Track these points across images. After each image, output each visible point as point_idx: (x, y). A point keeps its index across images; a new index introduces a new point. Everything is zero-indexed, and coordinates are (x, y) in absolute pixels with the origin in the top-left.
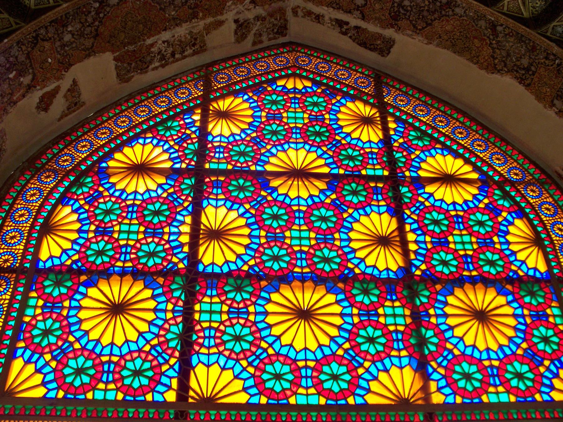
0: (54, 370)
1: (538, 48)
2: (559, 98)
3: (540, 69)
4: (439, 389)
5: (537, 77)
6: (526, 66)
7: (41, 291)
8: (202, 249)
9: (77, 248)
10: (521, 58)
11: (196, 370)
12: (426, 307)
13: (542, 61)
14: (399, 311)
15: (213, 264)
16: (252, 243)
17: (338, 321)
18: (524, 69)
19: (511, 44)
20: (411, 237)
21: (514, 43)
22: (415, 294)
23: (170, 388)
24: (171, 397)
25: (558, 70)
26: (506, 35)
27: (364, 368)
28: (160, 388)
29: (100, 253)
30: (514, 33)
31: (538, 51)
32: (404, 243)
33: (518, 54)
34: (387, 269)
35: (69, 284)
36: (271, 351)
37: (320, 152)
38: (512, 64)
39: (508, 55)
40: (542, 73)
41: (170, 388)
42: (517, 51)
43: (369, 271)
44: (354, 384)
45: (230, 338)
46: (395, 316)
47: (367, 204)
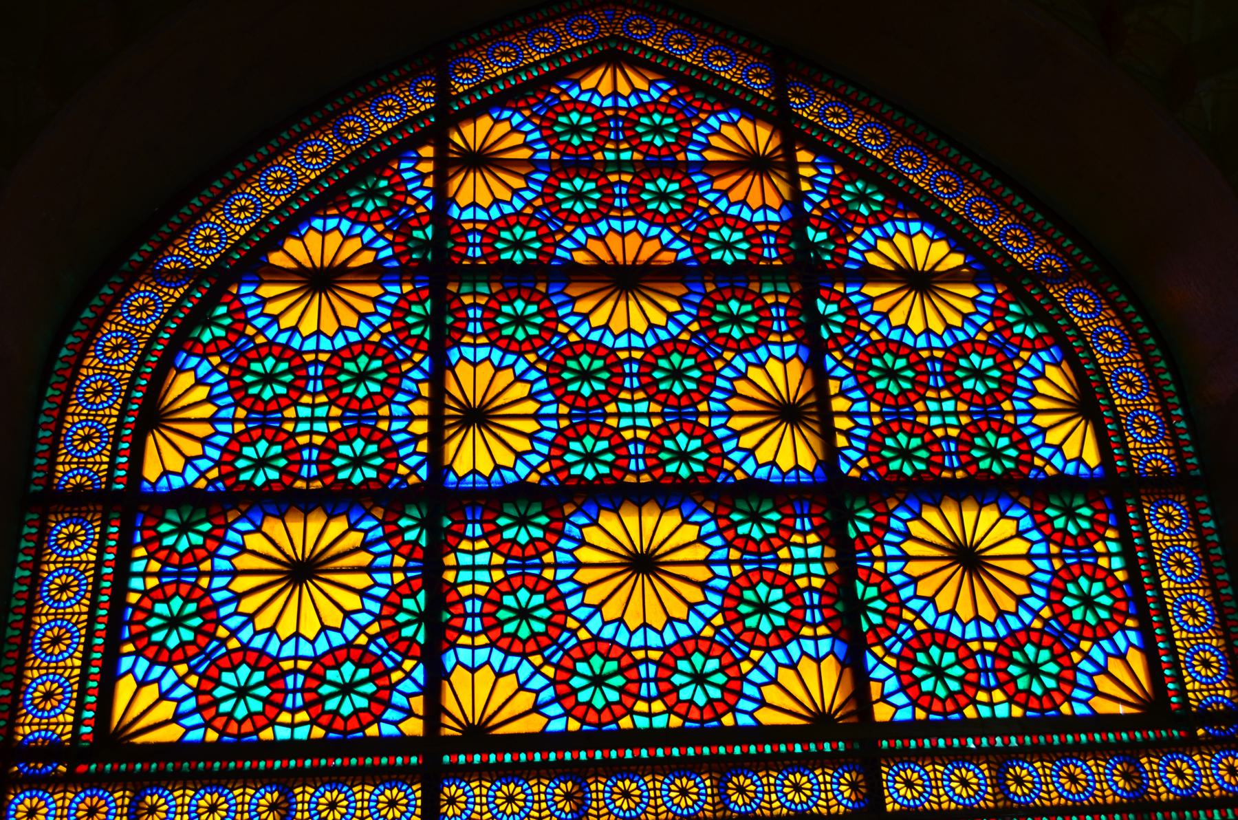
0: (196, 692)
4: (884, 698)
8: (451, 447)
9: (215, 454)
11: (452, 678)
14: (815, 552)
15: (474, 471)
16: (543, 428)
17: (701, 573)
20: (839, 404)
23: (409, 713)
27: (751, 661)
28: (391, 714)
29: (261, 463)
32: (826, 416)
34: (797, 467)
35: (206, 527)
36: (583, 635)
43: (762, 473)
44: (733, 691)
45: (511, 615)
46: (807, 561)
47: (759, 341)
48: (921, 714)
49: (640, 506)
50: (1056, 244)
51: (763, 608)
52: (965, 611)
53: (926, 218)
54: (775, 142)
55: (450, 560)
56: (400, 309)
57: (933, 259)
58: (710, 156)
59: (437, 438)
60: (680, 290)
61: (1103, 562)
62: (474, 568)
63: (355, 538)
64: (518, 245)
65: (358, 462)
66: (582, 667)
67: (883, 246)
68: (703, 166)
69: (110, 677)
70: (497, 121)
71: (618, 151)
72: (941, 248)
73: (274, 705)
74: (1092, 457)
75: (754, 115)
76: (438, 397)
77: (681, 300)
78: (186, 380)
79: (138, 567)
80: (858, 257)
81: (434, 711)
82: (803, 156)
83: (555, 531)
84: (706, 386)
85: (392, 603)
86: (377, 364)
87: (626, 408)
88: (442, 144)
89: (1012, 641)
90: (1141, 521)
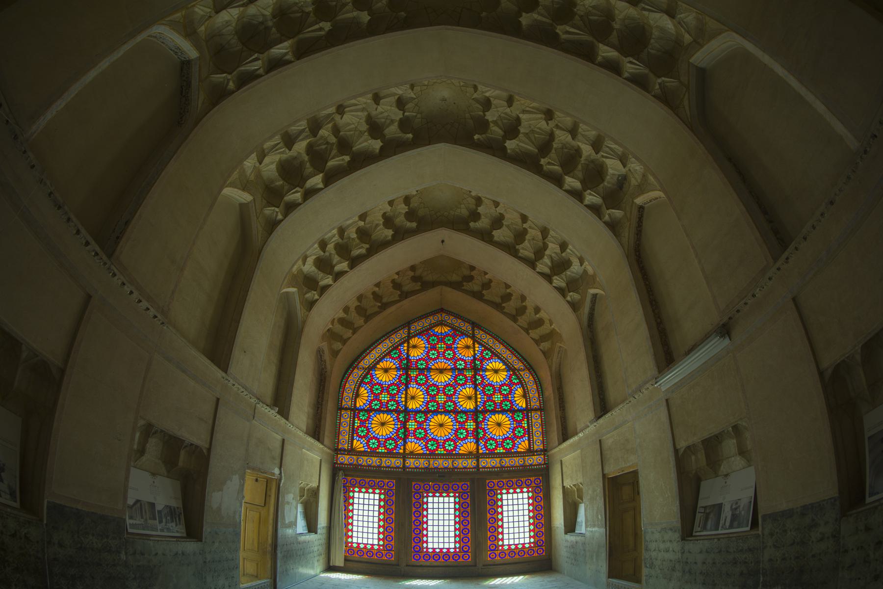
7: (359, 418)
12: (481, 422)
14: (472, 424)
17: (451, 427)
20: (479, 396)
22: (478, 417)
23: (401, 449)
24: (401, 451)
28: (398, 449)
32: (476, 398)
37: (449, 363)
41: (401, 449)
48: (487, 452)
49: (441, 415)
50: (523, 363)
51: (462, 434)
52: (497, 434)
53: (499, 358)
54: (472, 342)
55: (408, 424)
56: (400, 377)
57: (499, 367)
58: (459, 346)
59: (406, 401)
60: (451, 374)
61: (523, 425)
62: (412, 425)
63: (392, 419)
64: (422, 364)
65: (392, 405)
66: (429, 443)
67: (490, 364)
68: (457, 348)
69: (353, 439)
70: (419, 338)
71: (441, 345)
72: (501, 364)
73: (379, 446)
74: (524, 406)
75: (468, 336)
76: (406, 394)
77: (451, 376)
78: (363, 389)
79: (356, 422)
80: (485, 367)
81: (405, 449)
82: (477, 345)
83: (426, 419)
84: (455, 393)
85: (398, 430)
86: (396, 387)
87: (440, 397)
88: (409, 343)
89: (506, 439)
90: (531, 417)
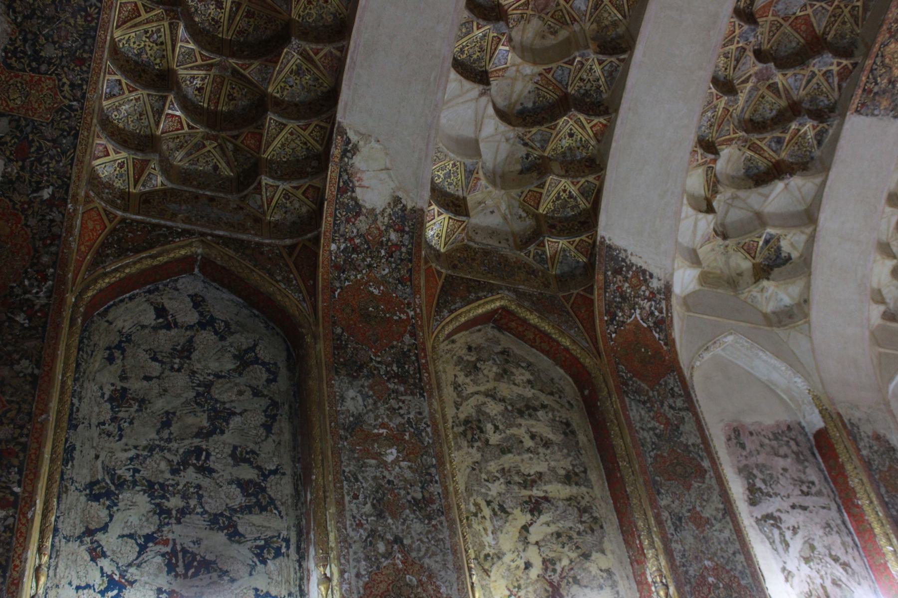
1: (85, 69)
2: (14, 124)
3: (49, 79)
5: (32, 77)
6: (42, 54)
10: (54, 43)
13: (65, 80)
18: (36, 52)
19: (72, 21)
21: (75, 27)
25: (61, 110)
26: (85, 10)
30: (94, 24)
31: (78, 68)
33: (60, 37)
38: (35, 29)
39: (50, 20)
40: (44, 85)
42: (63, 34)
